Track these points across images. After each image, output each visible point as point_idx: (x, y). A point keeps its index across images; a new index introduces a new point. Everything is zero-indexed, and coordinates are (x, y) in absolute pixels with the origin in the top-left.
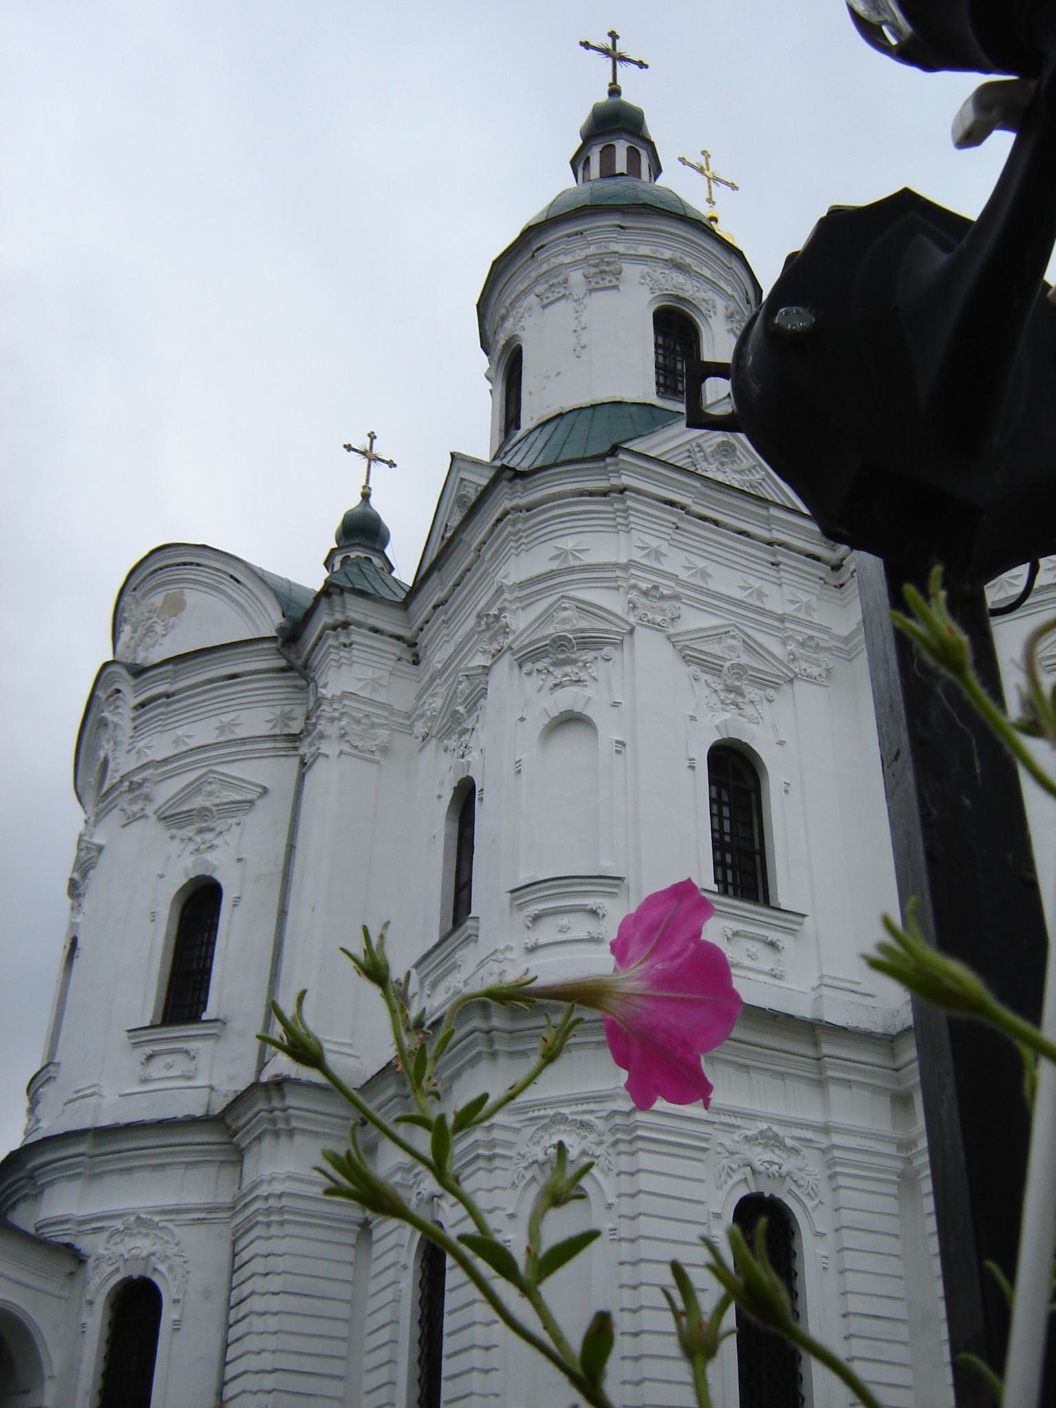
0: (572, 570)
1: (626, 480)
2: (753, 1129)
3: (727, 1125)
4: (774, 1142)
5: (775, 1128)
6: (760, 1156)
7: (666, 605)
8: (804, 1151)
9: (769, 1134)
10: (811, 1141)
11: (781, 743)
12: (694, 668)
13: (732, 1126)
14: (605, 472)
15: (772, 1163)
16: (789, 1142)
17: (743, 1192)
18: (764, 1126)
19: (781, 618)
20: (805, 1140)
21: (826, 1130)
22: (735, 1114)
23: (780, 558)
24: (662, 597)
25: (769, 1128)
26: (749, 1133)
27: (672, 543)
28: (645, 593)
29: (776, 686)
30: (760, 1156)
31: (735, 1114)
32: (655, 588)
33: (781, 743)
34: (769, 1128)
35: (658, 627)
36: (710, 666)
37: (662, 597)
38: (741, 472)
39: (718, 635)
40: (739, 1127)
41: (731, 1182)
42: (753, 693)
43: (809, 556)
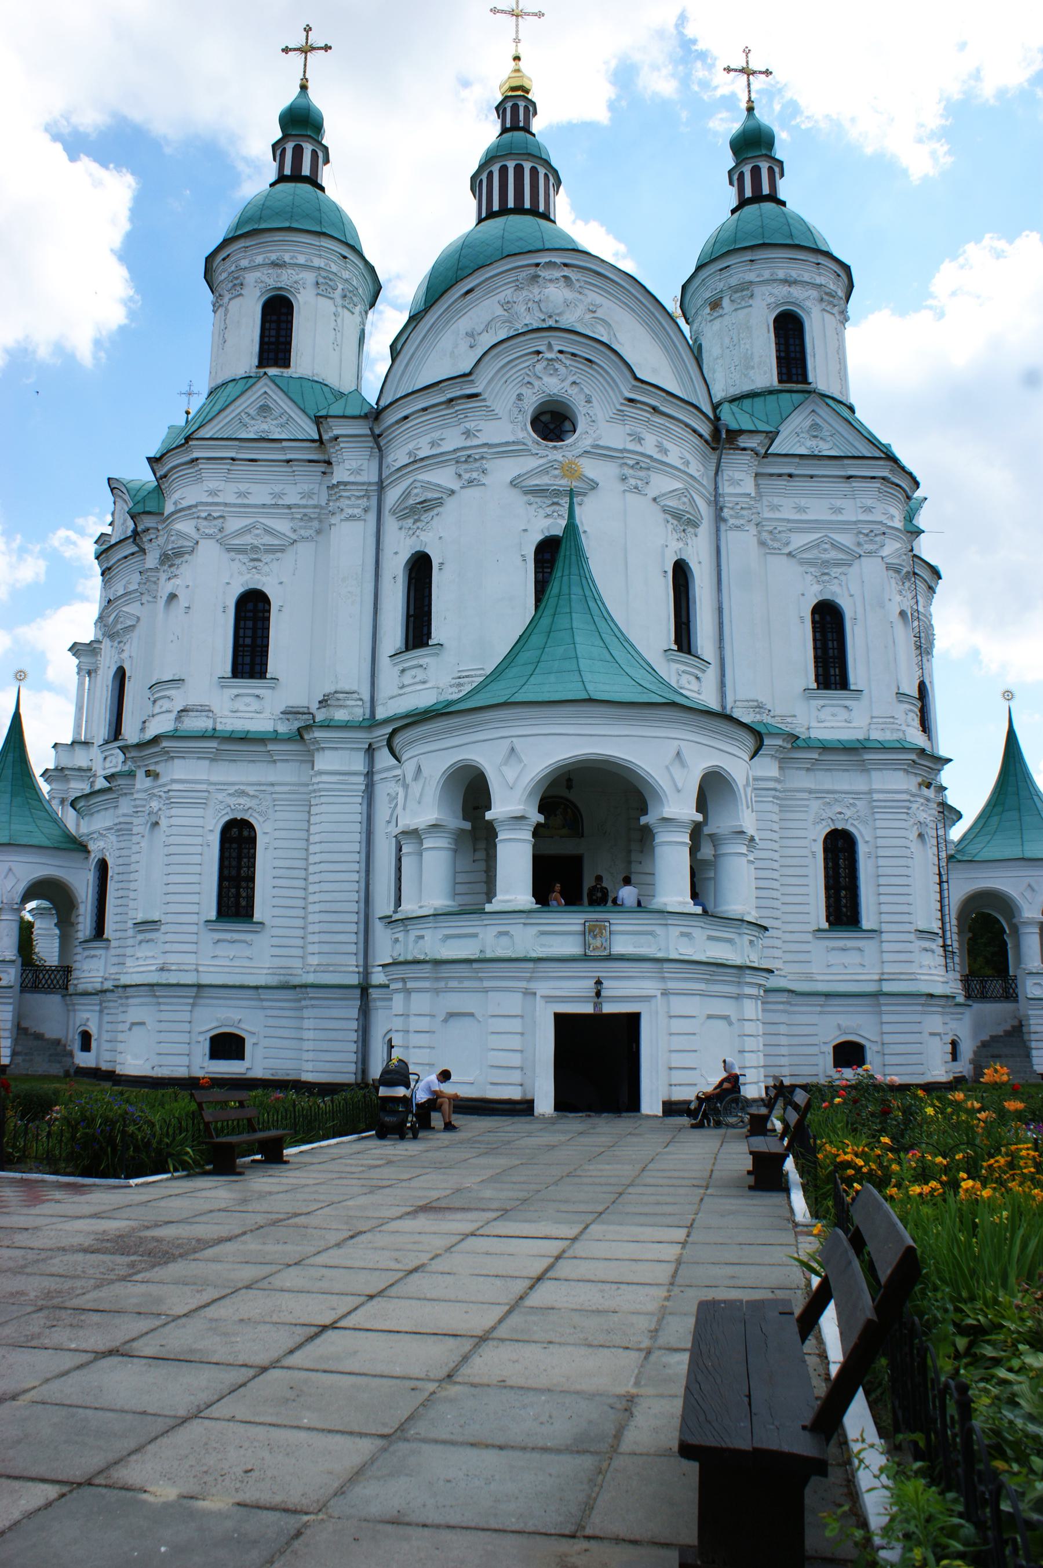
0: (181, 510)
1: (195, 455)
4: (243, 793)
5: (242, 787)
6: (232, 801)
8: (261, 796)
11: (281, 583)
12: (233, 554)
14: (186, 452)
16: (252, 793)
17: (227, 818)
18: (237, 787)
19: (289, 507)
21: (273, 785)
22: (224, 784)
23: (295, 468)
24: (215, 518)
27: (227, 480)
28: (206, 518)
29: (282, 551)
30: (232, 801)
31: (224, 784)
32: (209, 515)
35: (209, 536)
36: (240, 550)
37: (215, 518)
38: (276, 419)
39: (247, 530)
42: (267, 558)
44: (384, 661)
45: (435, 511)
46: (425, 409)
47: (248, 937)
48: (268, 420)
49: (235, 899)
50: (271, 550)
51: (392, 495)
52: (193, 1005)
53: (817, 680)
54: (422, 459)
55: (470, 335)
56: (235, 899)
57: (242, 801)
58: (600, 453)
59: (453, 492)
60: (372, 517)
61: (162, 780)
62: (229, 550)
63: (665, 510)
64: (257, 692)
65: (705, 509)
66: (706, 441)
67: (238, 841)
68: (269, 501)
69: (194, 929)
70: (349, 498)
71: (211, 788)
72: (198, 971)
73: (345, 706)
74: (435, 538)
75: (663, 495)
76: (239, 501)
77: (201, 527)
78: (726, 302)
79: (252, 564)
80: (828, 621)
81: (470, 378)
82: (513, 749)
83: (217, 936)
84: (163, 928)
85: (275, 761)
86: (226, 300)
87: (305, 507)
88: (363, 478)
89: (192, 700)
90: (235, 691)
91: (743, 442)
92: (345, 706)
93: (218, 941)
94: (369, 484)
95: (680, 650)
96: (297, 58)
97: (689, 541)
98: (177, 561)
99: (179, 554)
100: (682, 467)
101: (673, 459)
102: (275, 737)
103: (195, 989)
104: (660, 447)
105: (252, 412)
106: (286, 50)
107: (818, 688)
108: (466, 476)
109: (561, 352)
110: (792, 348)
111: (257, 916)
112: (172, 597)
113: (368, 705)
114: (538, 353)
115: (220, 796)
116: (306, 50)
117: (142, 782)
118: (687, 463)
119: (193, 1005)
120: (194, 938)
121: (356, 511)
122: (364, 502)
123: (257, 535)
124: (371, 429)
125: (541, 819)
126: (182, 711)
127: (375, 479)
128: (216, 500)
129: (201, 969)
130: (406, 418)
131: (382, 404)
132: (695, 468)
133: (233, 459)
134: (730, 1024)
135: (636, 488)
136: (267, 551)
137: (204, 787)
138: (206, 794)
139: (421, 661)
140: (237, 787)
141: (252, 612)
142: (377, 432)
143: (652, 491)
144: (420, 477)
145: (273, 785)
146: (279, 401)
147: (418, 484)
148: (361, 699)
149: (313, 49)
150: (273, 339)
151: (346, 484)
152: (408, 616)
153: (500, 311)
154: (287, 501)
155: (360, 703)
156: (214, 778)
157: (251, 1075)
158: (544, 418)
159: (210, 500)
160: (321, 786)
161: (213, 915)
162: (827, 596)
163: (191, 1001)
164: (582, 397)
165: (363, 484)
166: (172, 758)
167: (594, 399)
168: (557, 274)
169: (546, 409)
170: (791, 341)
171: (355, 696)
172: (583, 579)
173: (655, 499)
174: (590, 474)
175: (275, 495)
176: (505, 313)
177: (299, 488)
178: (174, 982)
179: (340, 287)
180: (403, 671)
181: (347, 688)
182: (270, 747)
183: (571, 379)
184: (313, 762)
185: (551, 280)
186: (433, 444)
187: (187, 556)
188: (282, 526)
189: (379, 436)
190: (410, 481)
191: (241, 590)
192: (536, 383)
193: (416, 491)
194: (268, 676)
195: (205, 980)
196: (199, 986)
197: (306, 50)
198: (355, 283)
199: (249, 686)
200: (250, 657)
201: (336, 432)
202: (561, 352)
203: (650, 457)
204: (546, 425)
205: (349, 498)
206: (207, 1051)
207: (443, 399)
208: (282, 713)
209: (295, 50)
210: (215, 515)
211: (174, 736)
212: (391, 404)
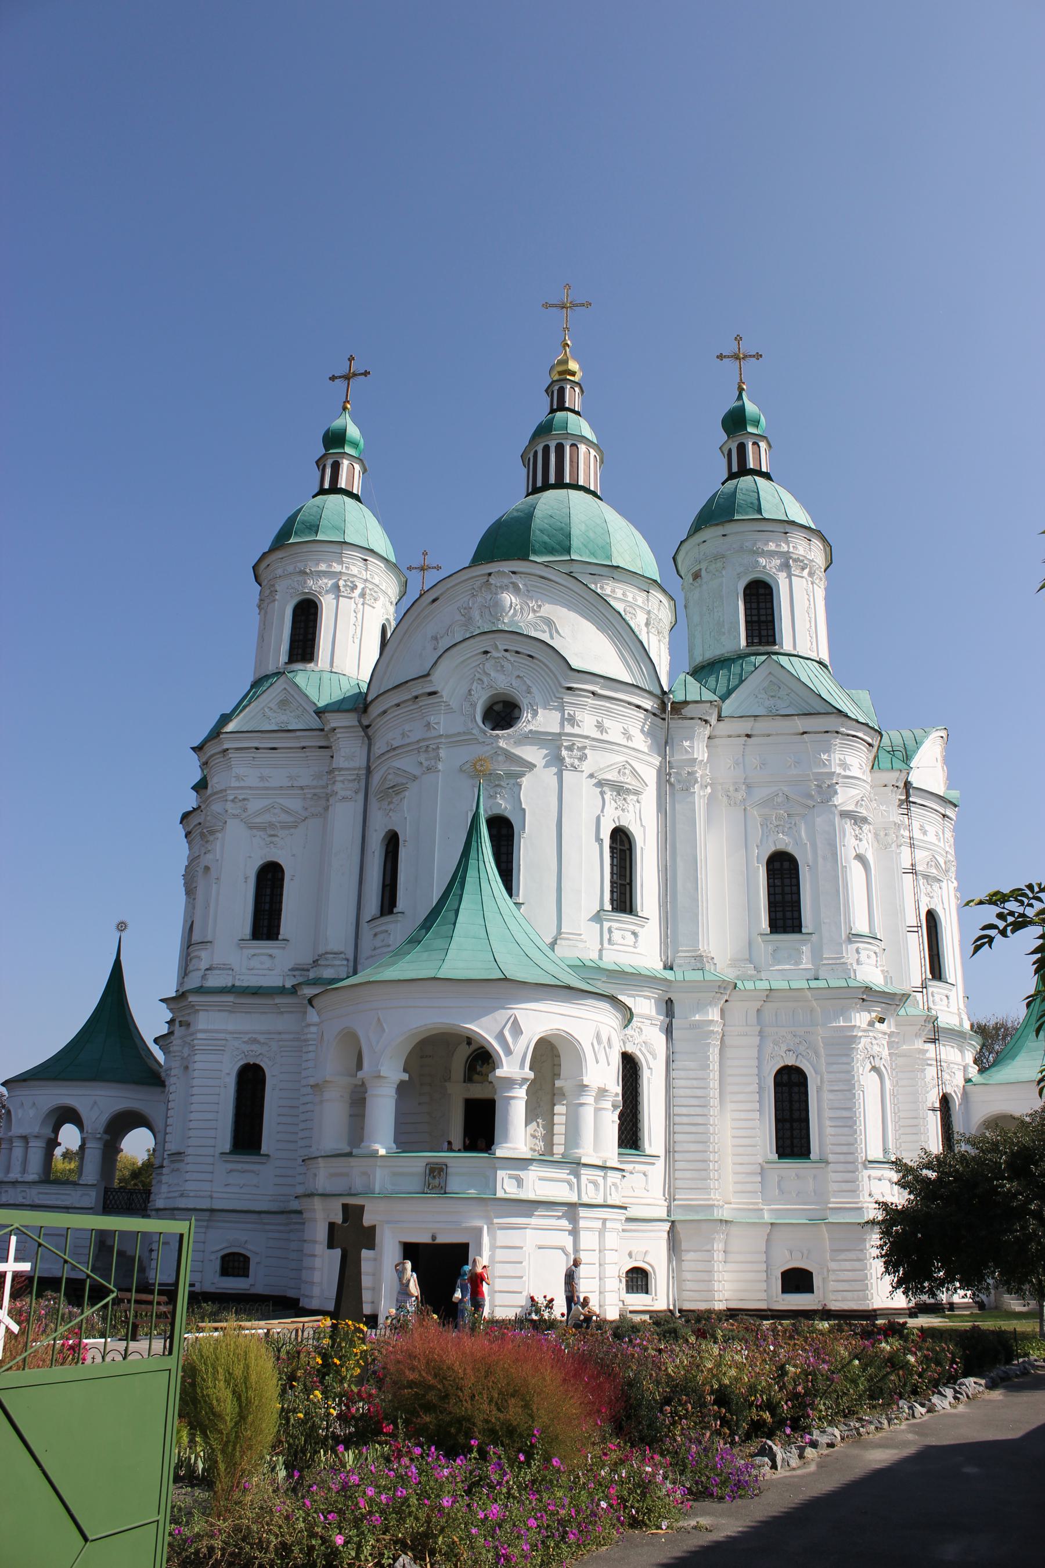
1: (226, 746)
2: (246, 1038)
4: (255, 1041)
5: (254, 1036)
6: (246, 1048)
7: (240, 804)
11: (294, 855)
16: (262, 1041)
17: (242, 1063)
18: (250, 1036)
19: (302, 788)
21: (280, 1033)
28: (233, 801)
33: (294, 855)
35: (235, 816)
43: (321, 747)
44: (364, 927)
45: (402, 796)
46: (398, 705)
48: (288, 712)
49: (247, 1136)
50: (285, 826)
51: (376, 778)
53: (770, 926)
54: (394, 749)
55: (435, 638)
56: (247, 1136)
57: (254, 1047)
58: (536, 738)
59: (415, 778)
60: (361, 796)
61: (192, 1029)
62: (251, 828)
63: (600, 784)
64: (270, 951)
65: (650, 775)
66: (654, 714)
67: (251, 1082)
68: (286, 783)
70: (343, 782)
71: (228, 1036)
72: (211, 1197)
73: (333, 966)
74: (404, 818)
75: (601, 770)
76: (261, 784)
77: (230, 811)
78: (703, 573)
79: (270, 839)
80: (783, 871)
81: (428, 679)
82: (379, 1019)
83: (230, 1166)
84: (188, 1159)
85: (282, 1013)
86: (265, 604)
87: (315, 787)
88: (352, 764)
89: (217, 960)
90: (252, 952)
91: (687, 711)
92: (333, 966)
93: (231, 1171)
94: (359, 769)
95: (614, 909)
96: (340, 384)
97: (631, 808)
98: (211, 838)
99: (212, 832)
100: (624, 742)
101: (614, 733)
102: (281, 991)
103: (208, 1213)
104: (600, 726)
105: (272, 705)
106: (333, 378)
107: (771, 932)
108: (425, 763)
109: (506, 650)
110: (763, 612)
111: (264, 1150)
112: (207, 869)
113: (351, 964)
114: (486, 652)
116: (347, 378)
117: (179, 1031)
118: (629, 738)
119: (207, 1227)
121: (348, 793)
122: (355, 785)
123: (275, 814)
124: (359, 721)
125: (405, 1077)
126: (207, 969)
127: (364, 764)
128: (242, 784)
129: (215, 1195)
130: (385, 712)
131: (369, 699)
132: (641, 742)
133: (257, 749)
134: (567, 1254)
135: (572, 766)
136: (283, 828)
138: (224, 1042)
139: (384, 928)
141: (270, 879)
142: (365, 723)
143: (587, 767)
144: (397, 764)
145: (280, 1033)
146: (296, 696)
147: (391, 771)
148: (348, 960)
149: (355, 375)
150: (301, 637)
151: (340, 769)
152: (384, 886)
153: (458, 617)
154: (302, 782)
155: (345, 963)
156: (231, 1027)
157: (253, 1291)
158: (496, 708)
159: (237, 784)
160: (309, 1036)
161: (227, 1147)
162: (781, 847)
163: (205, 1224)
164: (524, 688)
165: (355, 769)
166: (198, 1010)
167: (534, 690)
168: (506, 581)
169: (496, 700)
170: (762, 605)
171: (342, 956)
172: (481, 863)
173: (591, 776)
174: (530, 760)
175: (290, 777)
176: (462, 618)
177: (305, 772)
178: (191, 1206)
179: (360, 586)
180: (375, 935)
181: (336, 950)
182: (278, 1000)
183: (517, 673)
184: (305, 1013)
185: (501, 587)
186: (403, 735)
187: (219, 835)
188: (294, 804)
189: (368, 727)
190: (385, 768)
191: (261, 862)
192: (485, 679)
193: (390, 777)
194: (280, 937)
196: (212, 1211)
197: (347, 378)
198: (376, 581)
199: (265, 946)
200: (266, 923)
201: (333, 725)
202: (506, 650)
203: (587, 737)
204: (498, 713)
205: (343, 782)
206: (218, 1268)
207: (410, 697)
208: (292, 970)
209: (340, 377)
210: (241, 797)
211: (200, 990)
212: (377, 697)
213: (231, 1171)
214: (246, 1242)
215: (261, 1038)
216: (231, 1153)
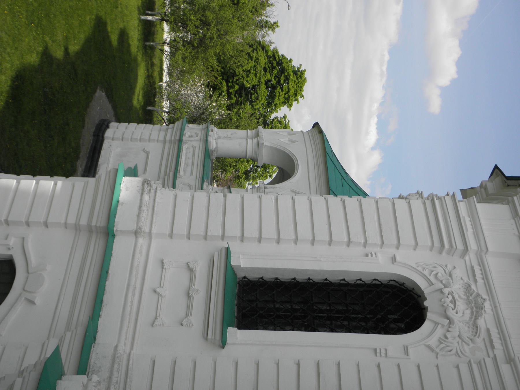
2: (480, 288)
3: (473, 271)
4: (476, 308)
5: (487, 305)
8: (479, 341)
9: (480, 300)
10: (493, 347)
13: (474, 276)
15: (454, 302)
16: (481, 322)
17: (422, 284)
20: (491, 341)
25: (485, 300)
26: (473, 287)
30: (457, 287)
34: (485, 300)
40: (476, 281)
41: (426, 273)
47: (197, 318)
52: (77, 228)
57: (461, 305)
69: (215, 230)
71: (471, 257)
72: (137, 233)
83: (201, 269)
93: (191, 271)
115: (460, 273)
120: (198, 229)
129: (141, 241)
137: (472, 244)
138: (460, 246)
140: (485, 296)
156: (491, 261)
163: (84, 222)
195: (121, 246)
196: (108, 234)
213: (191, 271)
214: (32, 302)
215: (486, 321)
216: (229, 270)
